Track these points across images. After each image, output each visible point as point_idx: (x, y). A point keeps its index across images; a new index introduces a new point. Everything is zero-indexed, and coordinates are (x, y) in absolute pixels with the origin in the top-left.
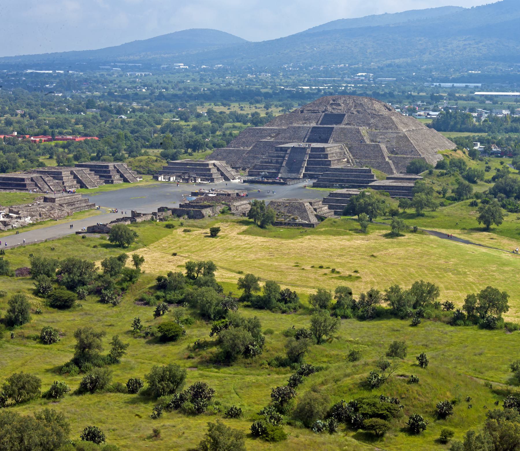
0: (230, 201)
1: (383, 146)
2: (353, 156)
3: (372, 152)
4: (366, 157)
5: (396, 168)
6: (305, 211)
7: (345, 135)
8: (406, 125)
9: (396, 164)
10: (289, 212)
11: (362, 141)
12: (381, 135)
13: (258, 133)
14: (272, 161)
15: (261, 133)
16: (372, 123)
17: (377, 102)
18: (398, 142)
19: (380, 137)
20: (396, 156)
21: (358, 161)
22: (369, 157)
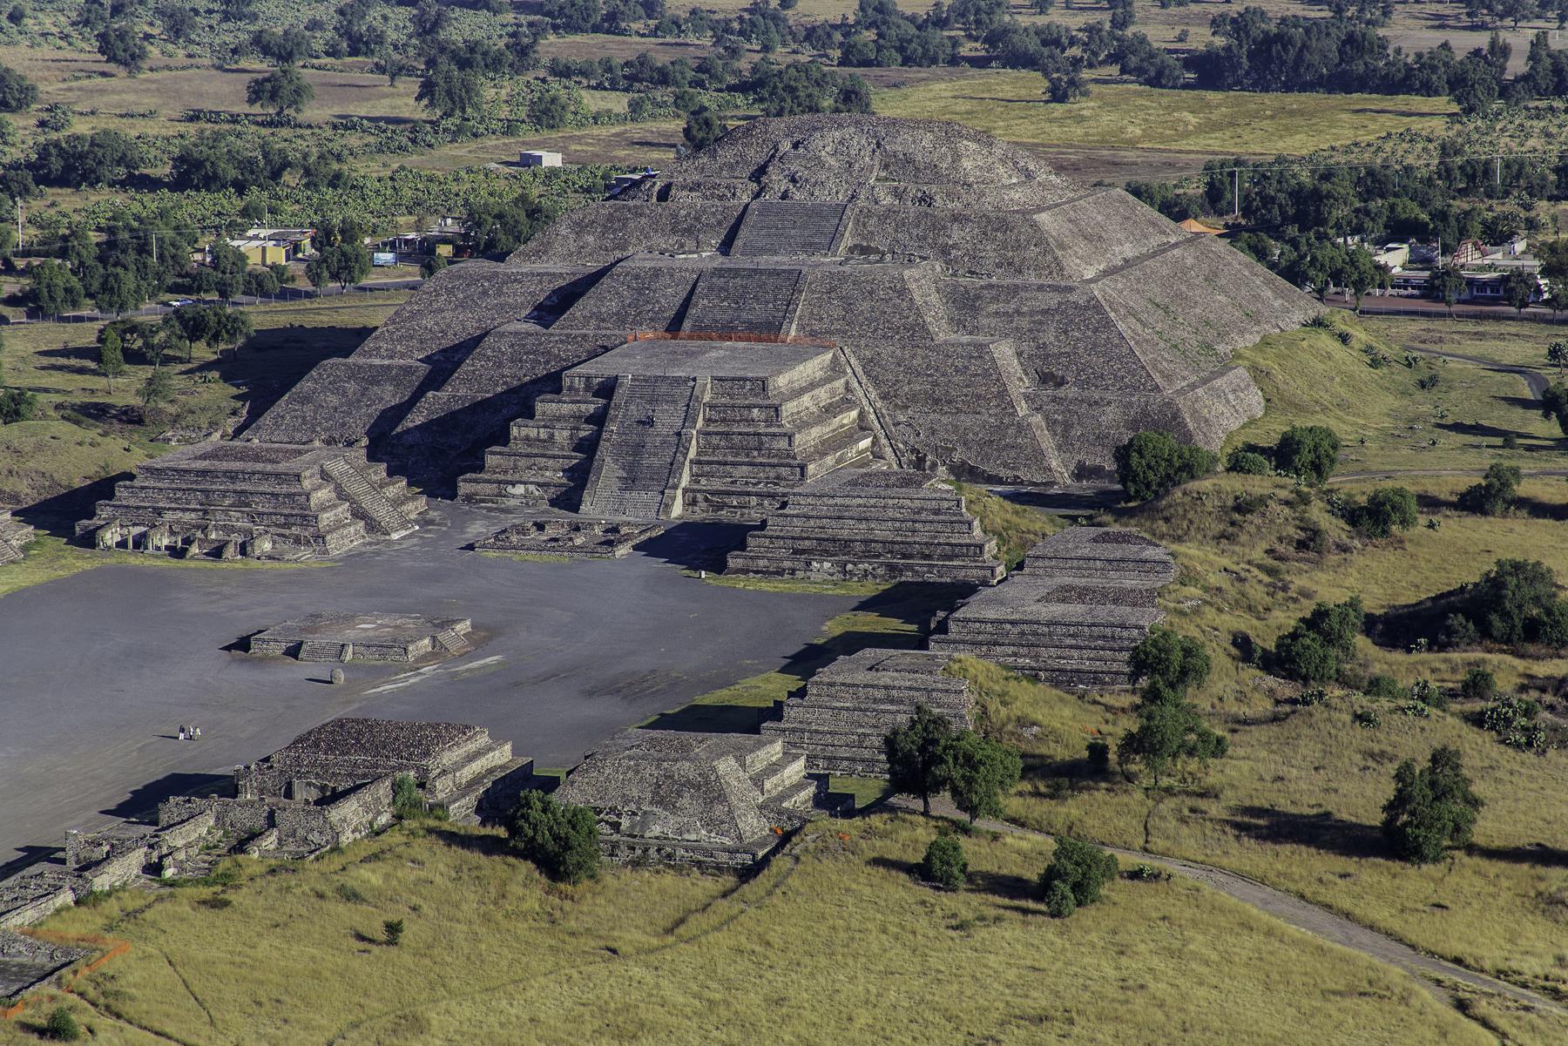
0: (427, 754)
1: (1005, 352)
2: (884, 397)
3: (957, 379)
4: (937, 401)
5: (1059, 448)
6: (721, 797)
7: (848, 305)
8: (1095, 239)
9: (1063, 431)
10: (660, 802)
11: (917, 332)
12: (995, 299)
13: (485, 293)
14: (552, 436)
15: (499, 293)
16: (954, 246)
17: (973, 146)
18: (1066, 332)
19: (993, 308)
20: (1061, 392)
21: (902, 418)
22: (950, 402)
